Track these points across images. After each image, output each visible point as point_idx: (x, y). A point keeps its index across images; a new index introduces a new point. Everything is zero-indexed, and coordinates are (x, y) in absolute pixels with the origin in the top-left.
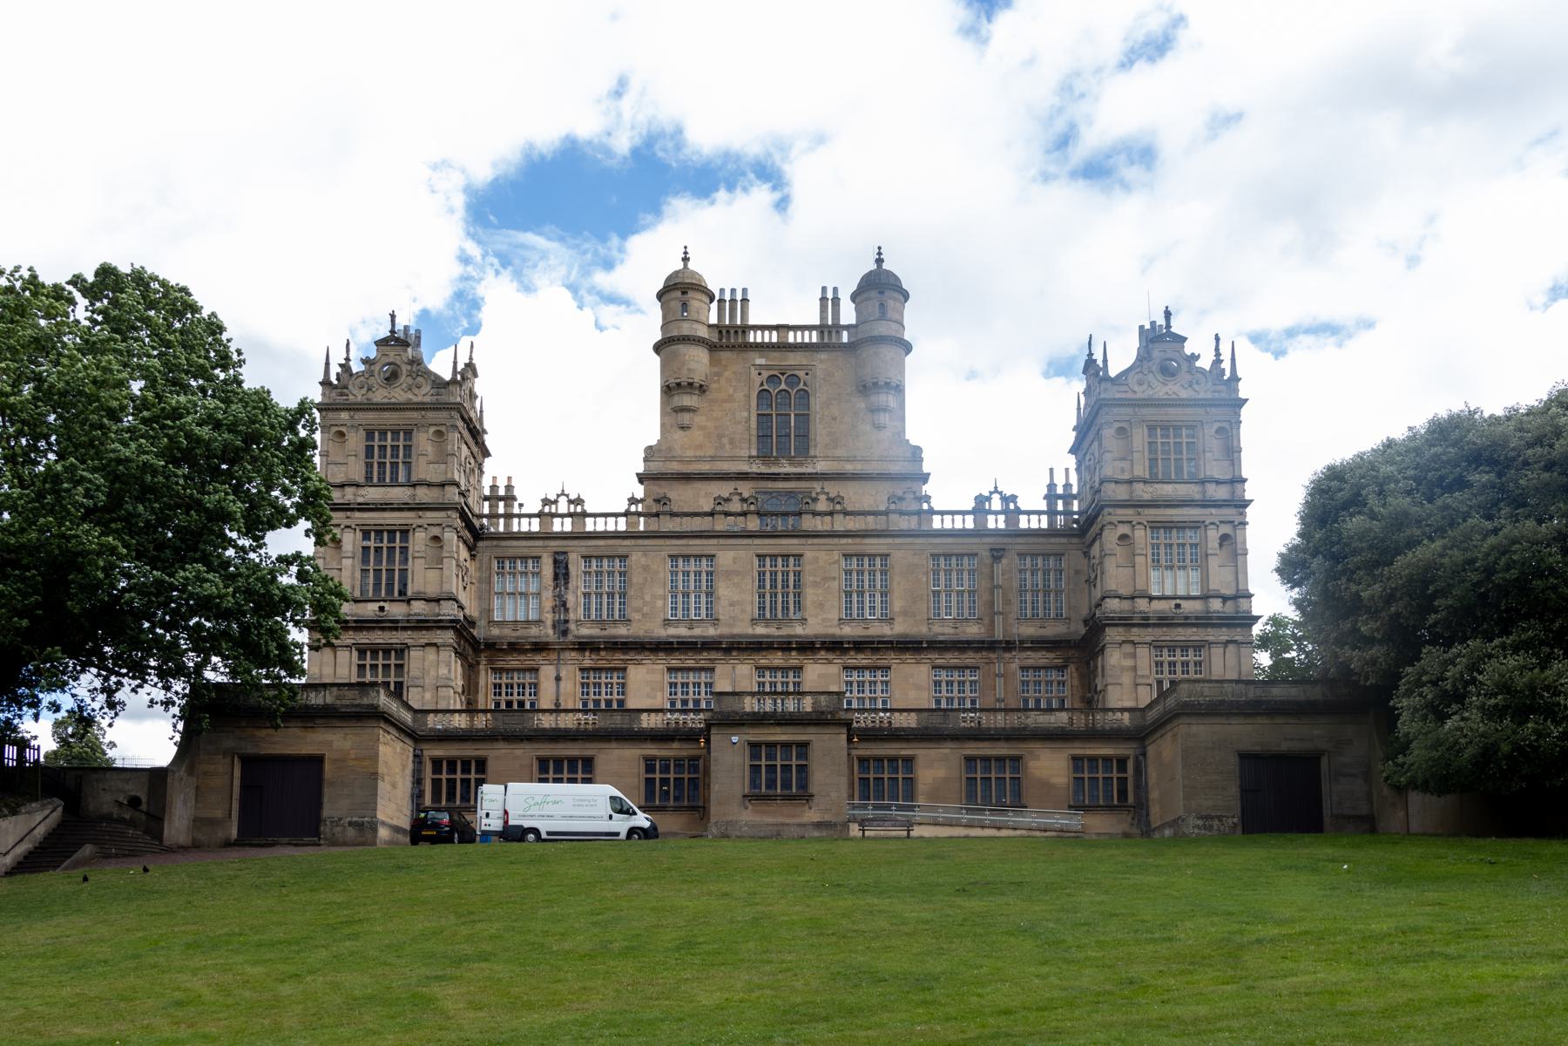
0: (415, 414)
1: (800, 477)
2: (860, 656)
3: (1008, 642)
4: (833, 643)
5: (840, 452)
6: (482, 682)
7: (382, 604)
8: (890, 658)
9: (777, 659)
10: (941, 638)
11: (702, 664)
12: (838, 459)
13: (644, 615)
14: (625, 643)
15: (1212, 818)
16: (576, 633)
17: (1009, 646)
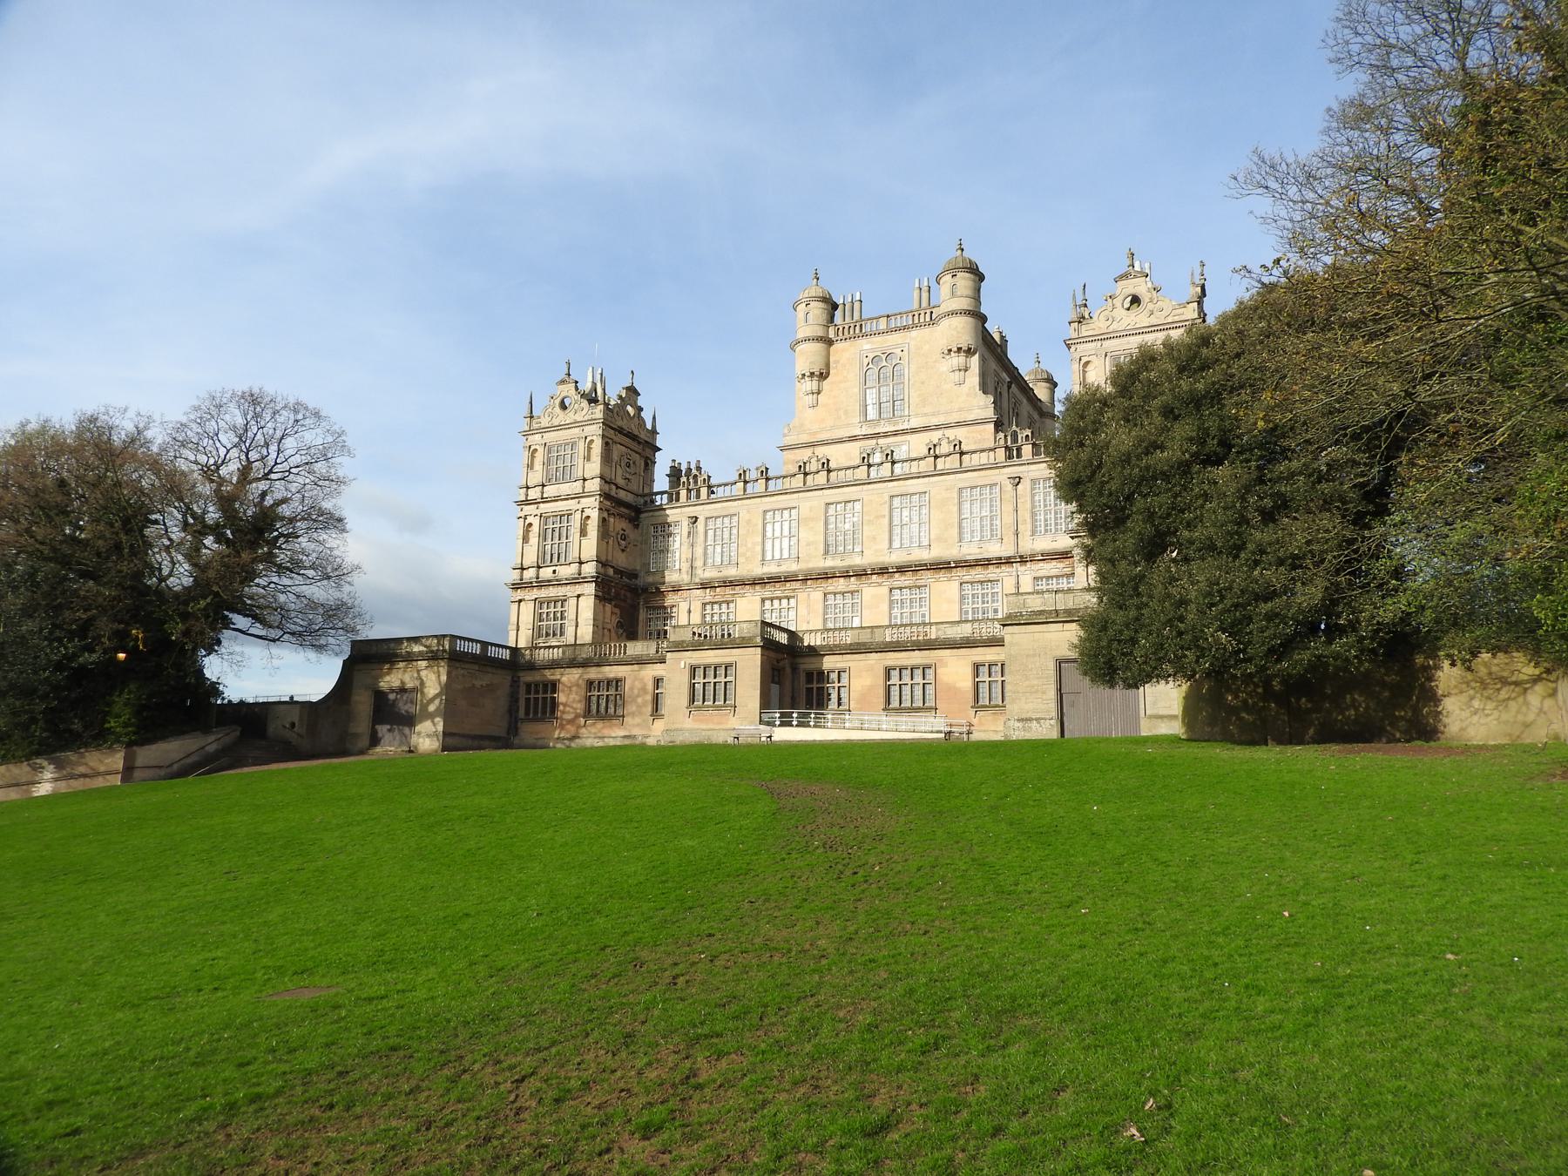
0: (577, 430)
1: (896, 434)
2: (903, 578)
3: (1021, 557)
4: (881, 569)
5: (928, 410)
6: (641, 618)
7: (554, 568)
8: (926, 577)
9: (841, 584)
10: (968, 558)
11: (787, 593)
12: (926, 415)
13: (747, 559)
14: (731, 582)
15: (1030, 720)
16: (702, 576)
17: (1023, 560)
